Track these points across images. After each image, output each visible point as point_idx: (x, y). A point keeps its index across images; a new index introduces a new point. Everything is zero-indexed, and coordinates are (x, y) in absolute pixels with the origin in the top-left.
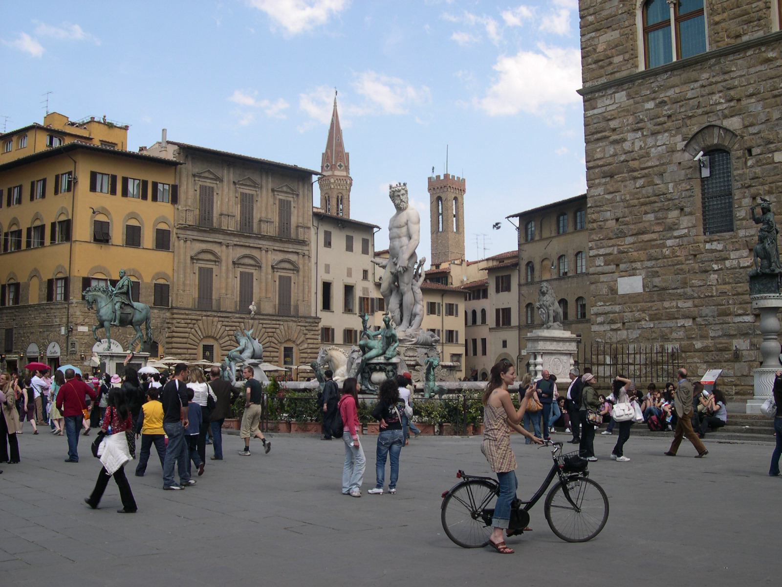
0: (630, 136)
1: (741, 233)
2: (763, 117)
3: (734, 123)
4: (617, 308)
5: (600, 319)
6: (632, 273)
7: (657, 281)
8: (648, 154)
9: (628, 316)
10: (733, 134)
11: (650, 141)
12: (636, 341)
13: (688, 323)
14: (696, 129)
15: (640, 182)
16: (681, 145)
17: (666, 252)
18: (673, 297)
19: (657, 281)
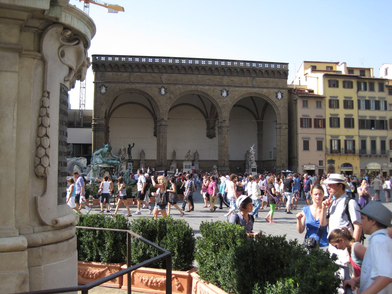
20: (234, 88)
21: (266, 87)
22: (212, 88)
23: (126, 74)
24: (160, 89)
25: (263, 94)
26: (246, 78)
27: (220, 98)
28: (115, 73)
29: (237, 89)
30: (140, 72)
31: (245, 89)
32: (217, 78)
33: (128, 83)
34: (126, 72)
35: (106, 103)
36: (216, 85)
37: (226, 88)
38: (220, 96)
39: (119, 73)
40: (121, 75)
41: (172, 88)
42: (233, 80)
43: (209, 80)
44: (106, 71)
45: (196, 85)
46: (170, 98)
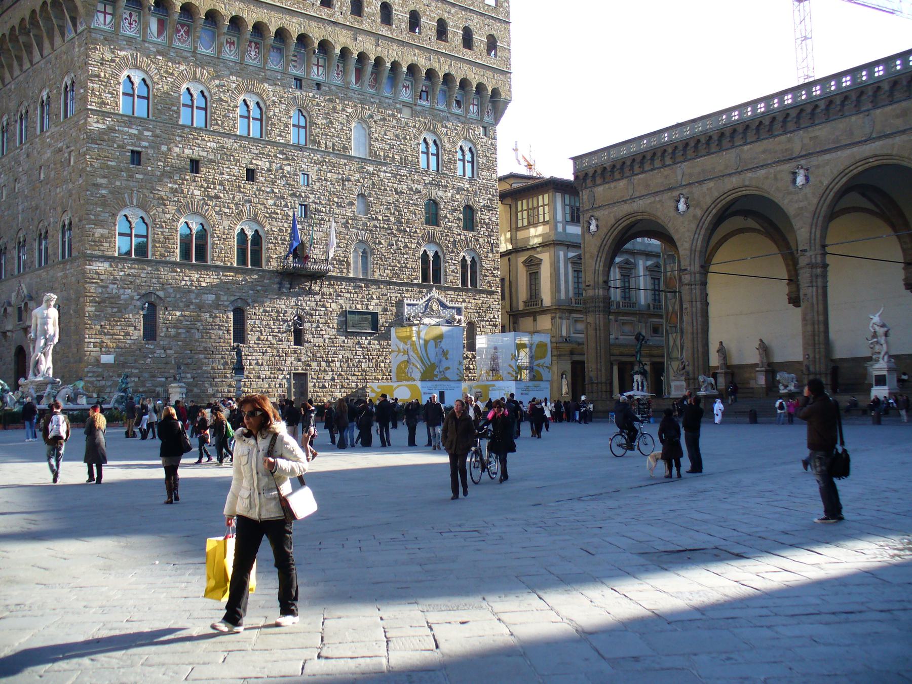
0: (111, 286)
1: (162, 343)
2: (173, 295)
3: (161, 294)
4: (100, 370)
5: (90, 375)
6: (108, 353)
7: (122, 358)
8: (119, 297)
9: (106, 374)
10: (160, 298)
11: (121, 291)
12: (110, 386)
13: (136, 379)
14: (143, 292)
15: (115, 310)
16: (137, 297)
17: (127, 346)
18: (129, 367)
19: (122, 358)
20: (820, 159)
21: (900, 129)
22: (772, 170)
23: (622, 184)
24: (678, 201)
25: (894, 153)
26: (847, 119)
27: (790, 193)
28: (607, 186)
29: (827, 157)
30: (645, 172)
31: (847, 152)
32: (779, 144)
33: (625, 201)
34: (623, 178)
35: (599, 252)
36: (779, 162)
37: (803, 162)
38: (791, 188)
39: (612, 185)
40: (615, 187)
41: (697, 191)
42: (816, 137)
43: (764, 152)
44: (595, 185)
45: (739, 173)
46: (694, 216)
